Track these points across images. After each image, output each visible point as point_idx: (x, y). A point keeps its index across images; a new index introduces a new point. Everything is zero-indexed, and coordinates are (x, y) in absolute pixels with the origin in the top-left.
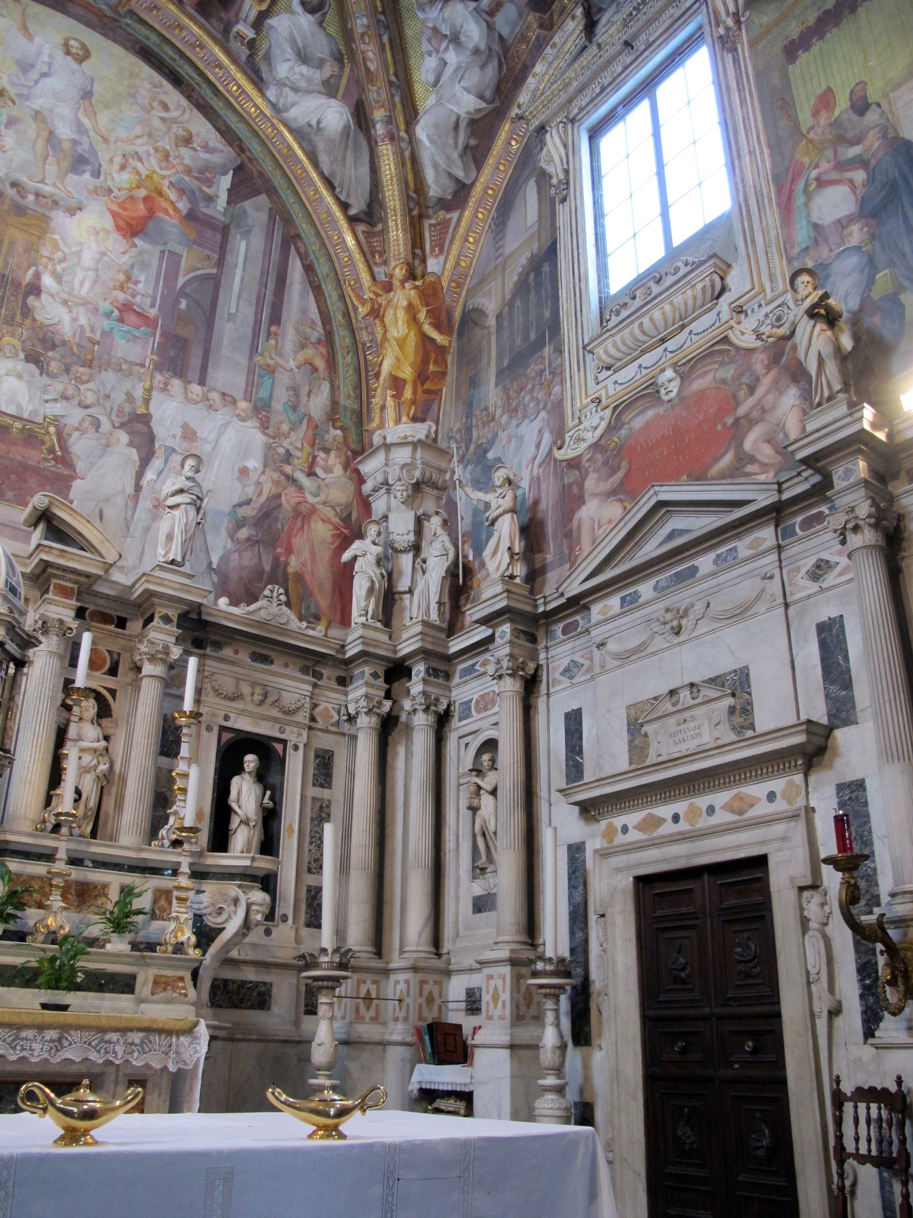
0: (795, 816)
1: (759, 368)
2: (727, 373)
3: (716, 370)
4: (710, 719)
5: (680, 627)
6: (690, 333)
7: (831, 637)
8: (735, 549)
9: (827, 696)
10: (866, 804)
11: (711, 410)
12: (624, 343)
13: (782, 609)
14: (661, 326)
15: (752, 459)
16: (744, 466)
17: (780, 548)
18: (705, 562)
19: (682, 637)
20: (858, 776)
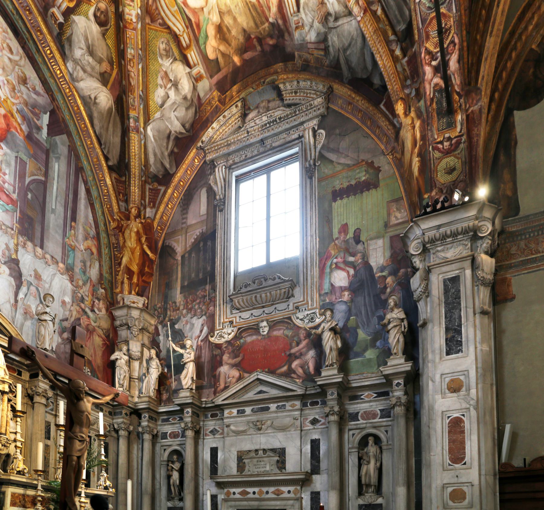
0: (297, 499)
1: (302, 338)
2: (289, 333)
3: (284, 330)
4: (270, 463)
5: (261, 428)
6: (275, 308)
7: (315, 445)
8: (285, 405)
9: (311, 464)
10: (320, 499)
11: (281, 346)
12: (247, 302)
13: (300, 432)
14: (264, 301)
15: (294, 372)
16: (291, 374)
17: (301, 410)
18: (273, 407)
19: (261, 432)
20: (318, 490)
